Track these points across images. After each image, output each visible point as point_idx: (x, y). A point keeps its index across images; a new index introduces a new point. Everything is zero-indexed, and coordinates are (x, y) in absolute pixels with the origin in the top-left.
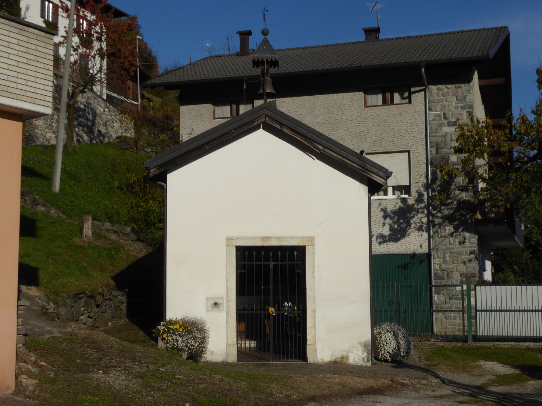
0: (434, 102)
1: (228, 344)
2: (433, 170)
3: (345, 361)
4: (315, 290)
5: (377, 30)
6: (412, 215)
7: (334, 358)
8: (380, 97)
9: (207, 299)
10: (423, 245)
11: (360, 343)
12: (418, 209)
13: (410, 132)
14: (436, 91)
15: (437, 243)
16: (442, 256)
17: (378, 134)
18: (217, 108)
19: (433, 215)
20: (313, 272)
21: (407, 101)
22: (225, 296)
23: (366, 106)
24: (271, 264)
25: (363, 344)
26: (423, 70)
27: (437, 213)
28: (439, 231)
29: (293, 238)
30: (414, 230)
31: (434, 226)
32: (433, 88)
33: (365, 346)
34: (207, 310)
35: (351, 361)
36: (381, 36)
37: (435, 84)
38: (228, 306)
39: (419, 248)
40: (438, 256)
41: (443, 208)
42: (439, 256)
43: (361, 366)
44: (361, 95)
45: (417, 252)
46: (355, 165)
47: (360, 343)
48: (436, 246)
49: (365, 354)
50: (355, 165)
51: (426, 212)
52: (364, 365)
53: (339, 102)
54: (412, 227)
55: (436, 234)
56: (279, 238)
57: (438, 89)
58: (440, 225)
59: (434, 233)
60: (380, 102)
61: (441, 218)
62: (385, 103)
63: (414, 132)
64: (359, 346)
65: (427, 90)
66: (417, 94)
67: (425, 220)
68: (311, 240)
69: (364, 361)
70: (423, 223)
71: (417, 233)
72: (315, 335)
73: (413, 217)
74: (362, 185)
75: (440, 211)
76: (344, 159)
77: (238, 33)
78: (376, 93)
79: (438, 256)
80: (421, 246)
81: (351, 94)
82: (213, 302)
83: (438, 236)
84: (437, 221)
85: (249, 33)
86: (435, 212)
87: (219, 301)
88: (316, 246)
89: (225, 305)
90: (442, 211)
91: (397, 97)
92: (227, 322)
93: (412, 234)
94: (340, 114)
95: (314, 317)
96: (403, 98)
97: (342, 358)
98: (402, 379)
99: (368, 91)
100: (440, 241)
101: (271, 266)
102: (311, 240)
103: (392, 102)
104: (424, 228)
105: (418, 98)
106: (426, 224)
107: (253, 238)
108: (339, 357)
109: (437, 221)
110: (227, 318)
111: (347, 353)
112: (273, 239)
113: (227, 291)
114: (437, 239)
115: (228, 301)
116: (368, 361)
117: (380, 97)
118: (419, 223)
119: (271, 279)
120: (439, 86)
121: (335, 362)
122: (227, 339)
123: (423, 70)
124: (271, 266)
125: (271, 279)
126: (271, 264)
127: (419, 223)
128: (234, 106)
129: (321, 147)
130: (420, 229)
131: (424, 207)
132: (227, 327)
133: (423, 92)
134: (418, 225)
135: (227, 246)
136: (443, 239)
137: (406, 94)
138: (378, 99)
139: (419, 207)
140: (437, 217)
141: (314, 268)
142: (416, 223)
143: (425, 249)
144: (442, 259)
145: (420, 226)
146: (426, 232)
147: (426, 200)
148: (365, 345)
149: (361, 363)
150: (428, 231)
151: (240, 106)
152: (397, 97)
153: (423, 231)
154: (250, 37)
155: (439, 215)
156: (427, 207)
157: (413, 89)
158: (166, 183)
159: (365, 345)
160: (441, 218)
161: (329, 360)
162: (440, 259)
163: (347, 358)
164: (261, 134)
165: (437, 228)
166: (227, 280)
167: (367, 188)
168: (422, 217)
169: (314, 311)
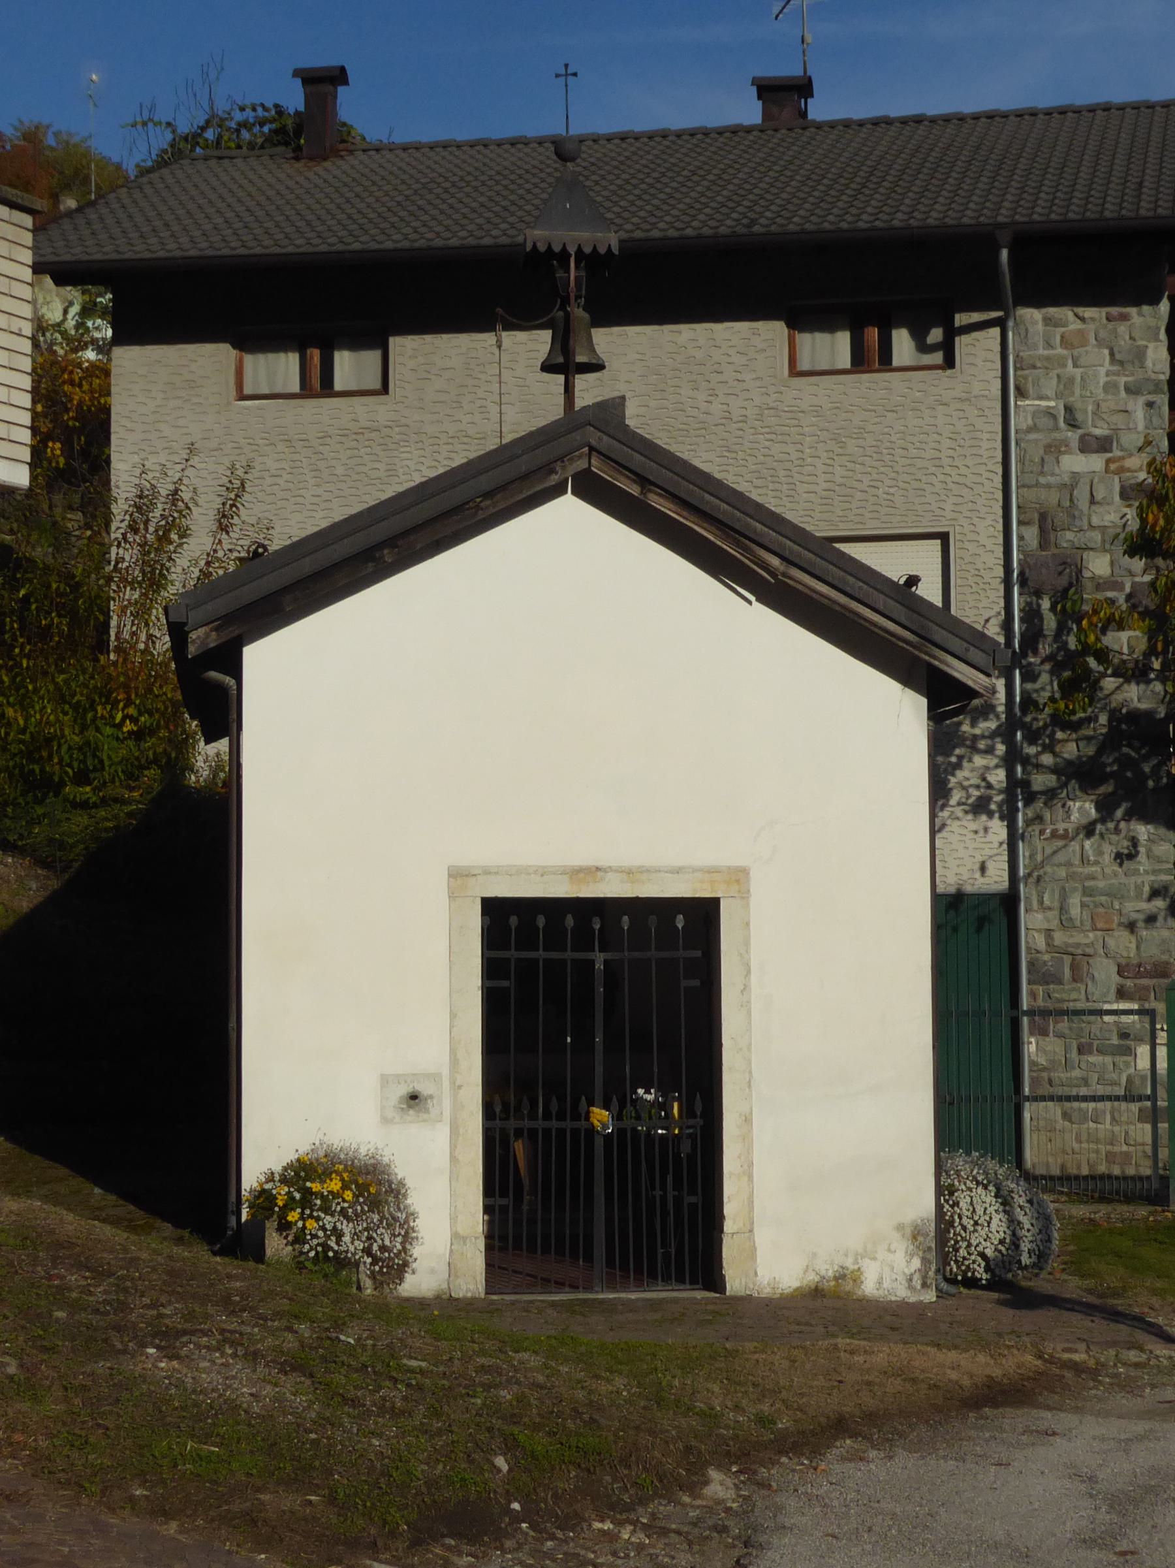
0: (1034, 367)
1: (455, 1236)
2: (1029, 604)
3: (848, 1286)
4: (749, 1049)
5: (804, 88)
6: (953, 759)
7: (812, 1278)
8: (843, 339)
9: (385, 1080)
10: (990, 865)
11: (900, 1227)
12: (975, 738)
13: (948, 470)
14: (1040, 327)
15: (1039, 858)
16: (1056, 904)
17: (839, 471)
18: (249, 359)
19: (1026, 761)
20: (746, 988)
21: (938, 358)
22: (445, 1072)
23: (795, 372)
24: (599, 959)
25: (908, 1231)
26: (1004, 254)
27: (1038, 754)
28: (1047, 816)
29: (678, 871)
30: (959, 811)
31: (1030, 799)
32: (1032, 316)
33: (914, 1238)
34: (385, 1120)
35: (869, 1287)
36: (819, 109)
37: (1038, 304)
38: (457, 1107)
39: (978, 875)
40: (1041, 902)
41: (1060, 735)
42: (1047, 902)
43: (903, 1304)
44: (775, 330)
45: (968, 889)
46: (891, 626)
47: (900, 1227)
48: (1035, 868)
49: (916, 1263)
50: (891, 626)
51: (1001, 748)
52: (912, 1300)
53: (699, 354)
54: (953, 801)
55: (1037, 828)
56: (629, 873)
57: (1047, 321)
58: (1050, 795)
59: (1028, 822)
60: (845, 361)
61: (1055, 770)
62: (860, 362)
63: (964, 470)
64: (896, 1235)
65: (1011, 324)
66: (975, 335)
67: (998, 777)
68: (739, 876)
69: (911, 1287)
70: (989, 786)
71: (971, 823)
72: (751, 1202)
73: (958, 766)
74: (909, 692)
75: (1049, 748)
76: (854, 605)
77: (297, 73)
78: (830, 327)
79: (1041, 902)
80: (983, 868)
81: (743, 327)
82: (404, 1090)
83: (1042, 832)
84: (1041, 781)
85: (339, 76)
86: (1031, 750)
87: (424, 1089)
88: (754, 901)
89: (447, 1104)
90: (1057, 749)
91: (902, 343)
92: (453, 1159)
93: (954, 826)
94: (702, 397)
95: (747, 1139)
96: (923, 347)
97: (841, 1277)
98: (1065, 1350)
99: (801, 319)
100: (1048, 851)
101: (599, 966)
102: (739, 876)
103: (885, 360)
104: (993, 807)
105: (979, 350)
106: (1000, 792)
107: (542, 872)
108: (830, 1273)
109: (1041, 781)
110: (453, 1147)
111: (856, 1262)
112: (610, 875)
113: (453, 1052)
114: (1039, 845)
115: (456, 1088)
116: (924, 1285)
117: (843, 339)
118: (978, 787)
119: (601, 1012)
120: (1052, 311)
121: (817, 1292)
122: (453, 1219)
123: (1004, 254)
124: (599, 966)
125: (601, 1012)
126: (599, 959)
127: (978, 787)
128: (315, 354)
129: (775, 562)
130: (980, 807)
131: (993, 735)
132: (453, 1177)
133: (996, 331)
134: (976, 793)
135: (452, 897)
136: (1060, 843)
137: (936, 335)
138: (836, 347)
139: (977, 731)
140: (1038, 766)
141: (749, 972)
142: (964, 788)
143: (997, 879)
144: (1056, 912)
145: (980, 798)
146: (1002, 818)
147: (1001, 709)
148: (916, 1234)
149: (902, 1293)
150: (1010, 818)
151: (338, 356)
152: (902, 343)
153: (990, 815)
154: (341, 90)
155: (1047, 759)
156: (1006, 732)
157: (961, 319)
158: (237, 674)
159: (916, 1234)
160: (1055, 770)
161: (795, 1284)
162: (1050, 914)
163: (856, 1277)
164: (568, 514)
165: (1039, 804)
166: (453, 1016)
167: (923, 702)
168: (987, 768)
169: (748, 1120)
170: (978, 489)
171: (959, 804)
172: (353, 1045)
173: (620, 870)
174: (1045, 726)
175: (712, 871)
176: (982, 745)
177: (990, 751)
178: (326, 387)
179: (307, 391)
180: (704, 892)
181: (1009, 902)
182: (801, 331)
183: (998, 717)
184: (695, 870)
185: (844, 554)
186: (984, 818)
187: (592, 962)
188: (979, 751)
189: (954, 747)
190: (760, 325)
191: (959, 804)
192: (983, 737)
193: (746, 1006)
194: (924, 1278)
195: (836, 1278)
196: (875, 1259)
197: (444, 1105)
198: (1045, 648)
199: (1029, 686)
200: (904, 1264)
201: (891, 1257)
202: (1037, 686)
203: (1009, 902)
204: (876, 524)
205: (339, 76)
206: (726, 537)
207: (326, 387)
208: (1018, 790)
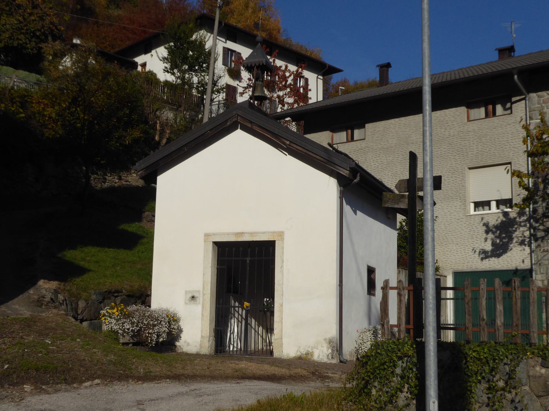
0: (535, 110)
1: (202, 336)
2: (535, 181)
3: (309, 357)
4: (283, 284)
5: (511, 49)
6: (514, 229)
7: (299, 354)
8: (483, 110)
9: (186, 292)
10: (525, 261)
11: (325, 340)
12: (521, 222)
13: (511, 144)
14: (536, 98)
15: (539, 258)
16: (545, 272)
17: (480, 147)
18: (335, 135)
19: (535, 229)
20: (282, 267)
21: (509, 111)
22: (201, 290)
23: (469, 120)
24: (248, 259)
25: (328, 341)
26: (516, 77)
27: (539, 226)
28: (542, 245)
29: (264, 233)
30: (516, 244)
31: (536, 240)
32: (533, 95)
33: (330, 343)
34: (186, 303)
35: (316, 357)
36: (517, 54)
37: (535, 91)
38: (204, 300)
39: (522, 264)
40: (540, 272)
41: (545, 220)
42: (542, 272)
43: (325, 364)
44: (462, 110)
45: (519, 268)
46: (318, 157)
47: (325, 340)
48: (539, 261)
49: (330, 351)
50: (318, 157)
51: (528, 225)
52: (328, 362)
53: (442, 119)
54: (514, 241)
55: (538, 249)
56: (251, 234)
57: (539, 96)
58: (543, 238)
59: (537, 247)
60: (483, 116)
61: (544, 231)
62: (487, 116)
63: (515, 143)
64: (324, 342)
65: (527, 98)
66: (518, 103)
67: (527, 234)
68: (281, 234)
69: (328, 358)
70: (525, 237)
71: (520, 248)
72: (282, 330)
73: (515, 231)
74: (331, 178)
75: (542, 224)
76: (308, 152)
77: (377, 66)
78: (479, 107)
79: (540, 272)
80: (523, 261)
81: (453, 110)
82: (190, 295)
83: (540, 250)
84: (540, 234)
85: (388, 65)
86: (537, 225)
87: (196, 295)
88: (285, 241)
89: (201, 299)
90: (545, 224)
91: (499, 109)
92: (202, 315)
93: (514, 249)
94: (443, 130)
95: (281, 312)
96: (505, 109)
97: (307, 354)
98: (332, 373)
99: (470, 106)
100: (542, 256)
101: (248, 261)
102: (281, 234)
103: (494, 114)
104: (526, 243)
105: (519, 108)
106: (528, 238)
107: (228, 234)
108: (304, 353)
109: (540, 234)
110: (202, 311)
111: (312, 350)
112: (246, 235)
113: (203, 285)
114: (539, 254)
115: (204, 295)
116: (332, 358)
117: (483, 110)
118: (521, 237)
120: (540, 93)
121: (300, 358)
122: (202, 332)
123: (516, 77)
124: (248, 261)
126: (248, 259)
127: (521, 237)
128: (350, 131)
129: (288, 143)
130: (522, 243)
131: (526, 221)
132: (202, 320)
133: (524, 101)
134: (521, 239)
135: (205, 241)
136: (545, 253)
137: (508, 105)
138: (482, 111)
139: (521, 220)
140: (539, 229)
141: (283, 262)
142: (517, 237)
143: (527, 265)
144: (545, 275)
145: (522, 240)
146: (529, 246)
147: (528, 213)
148: (330, 342)
149: (325, 360)
150: (530, 246)
151: (355, 131)
152: (499, 109)
153: (525, 245)
154: (390, 69)
155: (541, 227)
156: (528, 220)
157: (514, 99)
158: (156, 184)
159: (330, 342)
160: (544, 231)
161: (294, 355)
162: (543, 275)
163: (312, 354)
164: (239, 135)
165: (539, 242)
166: (204, 275)
167: (336, 180)
168: (524, 231)
169: (282, 305)
170: (519, 148)
171: (516, 242)
172: (181, 284)
173: (249, 233)
174: (541, 218)
175: (274, 233)
176: (522, 224)
177: (525, 226)
178: (352, 139)
179: (348, 141)
180: (271, 239)
181: (531, 271)
182: (471, 109)
183: (526, 215)
184: (269, 232)
185: (308, 139)
186: (523, 246)
187: (246, 260)
188: (522, 226)
189: (514, 225)
190: (458, 108)
191: (516, 242)
192: (523, 222)
193: (282, 272)
194: (332, 356)
195: (306, 354)
196: (317, 349)
197: (200, 300)
198: (540, 193)
199: (535, 206)
200: (326, 351)
201: (322, 348)
202: (538, 205)
203: (531, 271)
204: (491, 161)
205: (388, 65)
206: (276, 138)
207: (352, 139)
208: (534, 237)
